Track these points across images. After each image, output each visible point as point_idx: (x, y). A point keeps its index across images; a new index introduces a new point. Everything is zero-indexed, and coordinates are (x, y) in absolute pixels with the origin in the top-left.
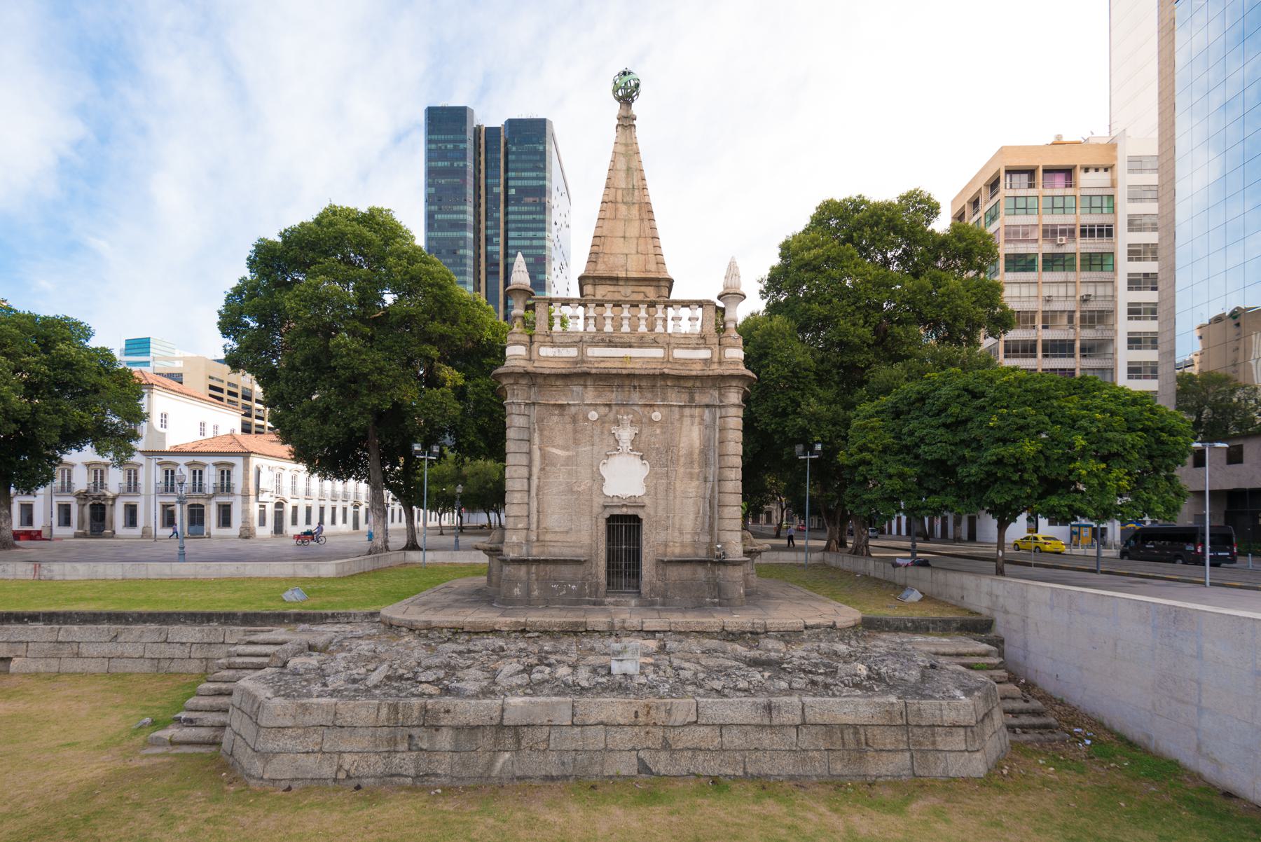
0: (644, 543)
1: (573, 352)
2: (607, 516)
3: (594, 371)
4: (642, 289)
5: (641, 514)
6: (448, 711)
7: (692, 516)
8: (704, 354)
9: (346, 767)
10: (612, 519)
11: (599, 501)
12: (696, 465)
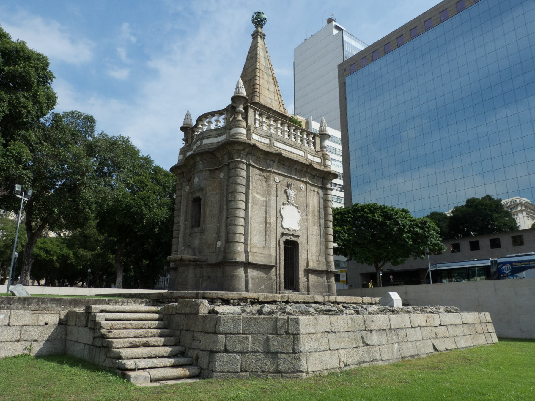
0: (300, 258)
2: (284, 240)
3: (285, 154)
5: (299, 240)
6: (372, 321)
7: (315, 246)
8: (318, 160)
9: (342, 359)
10: (286, 242)
11: (280, 230)
12: (316, 218)
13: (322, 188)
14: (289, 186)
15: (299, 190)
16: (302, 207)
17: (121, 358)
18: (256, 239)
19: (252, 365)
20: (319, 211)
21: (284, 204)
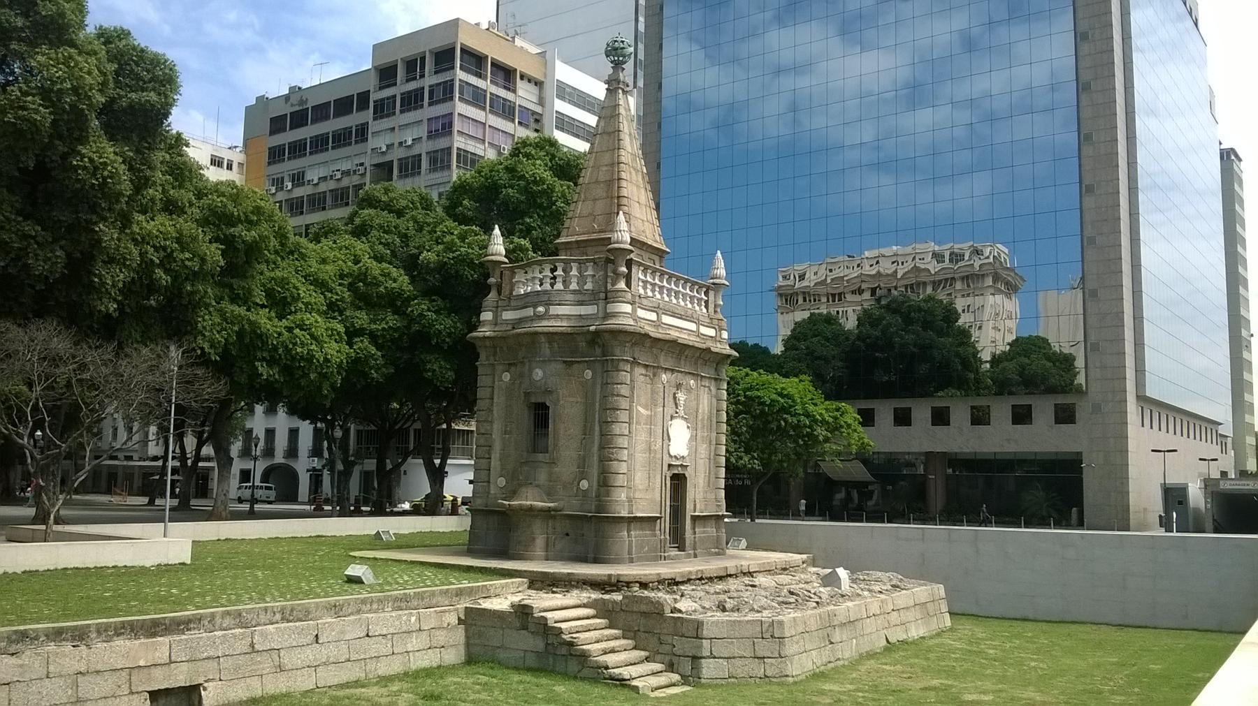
1: (653, 316)
4: (654, 257)
13: (716, 379)
14: (679, 386)
15: (689, 390)
16: (691, 419)
17: (607, 668)
18: (639, 478)
19: (739, 671)
20: (710, 419)
21: (672, 418)
